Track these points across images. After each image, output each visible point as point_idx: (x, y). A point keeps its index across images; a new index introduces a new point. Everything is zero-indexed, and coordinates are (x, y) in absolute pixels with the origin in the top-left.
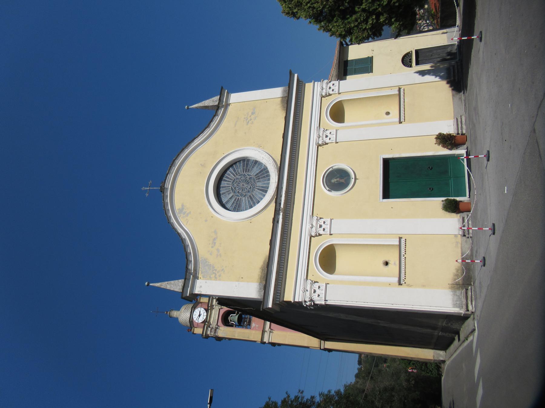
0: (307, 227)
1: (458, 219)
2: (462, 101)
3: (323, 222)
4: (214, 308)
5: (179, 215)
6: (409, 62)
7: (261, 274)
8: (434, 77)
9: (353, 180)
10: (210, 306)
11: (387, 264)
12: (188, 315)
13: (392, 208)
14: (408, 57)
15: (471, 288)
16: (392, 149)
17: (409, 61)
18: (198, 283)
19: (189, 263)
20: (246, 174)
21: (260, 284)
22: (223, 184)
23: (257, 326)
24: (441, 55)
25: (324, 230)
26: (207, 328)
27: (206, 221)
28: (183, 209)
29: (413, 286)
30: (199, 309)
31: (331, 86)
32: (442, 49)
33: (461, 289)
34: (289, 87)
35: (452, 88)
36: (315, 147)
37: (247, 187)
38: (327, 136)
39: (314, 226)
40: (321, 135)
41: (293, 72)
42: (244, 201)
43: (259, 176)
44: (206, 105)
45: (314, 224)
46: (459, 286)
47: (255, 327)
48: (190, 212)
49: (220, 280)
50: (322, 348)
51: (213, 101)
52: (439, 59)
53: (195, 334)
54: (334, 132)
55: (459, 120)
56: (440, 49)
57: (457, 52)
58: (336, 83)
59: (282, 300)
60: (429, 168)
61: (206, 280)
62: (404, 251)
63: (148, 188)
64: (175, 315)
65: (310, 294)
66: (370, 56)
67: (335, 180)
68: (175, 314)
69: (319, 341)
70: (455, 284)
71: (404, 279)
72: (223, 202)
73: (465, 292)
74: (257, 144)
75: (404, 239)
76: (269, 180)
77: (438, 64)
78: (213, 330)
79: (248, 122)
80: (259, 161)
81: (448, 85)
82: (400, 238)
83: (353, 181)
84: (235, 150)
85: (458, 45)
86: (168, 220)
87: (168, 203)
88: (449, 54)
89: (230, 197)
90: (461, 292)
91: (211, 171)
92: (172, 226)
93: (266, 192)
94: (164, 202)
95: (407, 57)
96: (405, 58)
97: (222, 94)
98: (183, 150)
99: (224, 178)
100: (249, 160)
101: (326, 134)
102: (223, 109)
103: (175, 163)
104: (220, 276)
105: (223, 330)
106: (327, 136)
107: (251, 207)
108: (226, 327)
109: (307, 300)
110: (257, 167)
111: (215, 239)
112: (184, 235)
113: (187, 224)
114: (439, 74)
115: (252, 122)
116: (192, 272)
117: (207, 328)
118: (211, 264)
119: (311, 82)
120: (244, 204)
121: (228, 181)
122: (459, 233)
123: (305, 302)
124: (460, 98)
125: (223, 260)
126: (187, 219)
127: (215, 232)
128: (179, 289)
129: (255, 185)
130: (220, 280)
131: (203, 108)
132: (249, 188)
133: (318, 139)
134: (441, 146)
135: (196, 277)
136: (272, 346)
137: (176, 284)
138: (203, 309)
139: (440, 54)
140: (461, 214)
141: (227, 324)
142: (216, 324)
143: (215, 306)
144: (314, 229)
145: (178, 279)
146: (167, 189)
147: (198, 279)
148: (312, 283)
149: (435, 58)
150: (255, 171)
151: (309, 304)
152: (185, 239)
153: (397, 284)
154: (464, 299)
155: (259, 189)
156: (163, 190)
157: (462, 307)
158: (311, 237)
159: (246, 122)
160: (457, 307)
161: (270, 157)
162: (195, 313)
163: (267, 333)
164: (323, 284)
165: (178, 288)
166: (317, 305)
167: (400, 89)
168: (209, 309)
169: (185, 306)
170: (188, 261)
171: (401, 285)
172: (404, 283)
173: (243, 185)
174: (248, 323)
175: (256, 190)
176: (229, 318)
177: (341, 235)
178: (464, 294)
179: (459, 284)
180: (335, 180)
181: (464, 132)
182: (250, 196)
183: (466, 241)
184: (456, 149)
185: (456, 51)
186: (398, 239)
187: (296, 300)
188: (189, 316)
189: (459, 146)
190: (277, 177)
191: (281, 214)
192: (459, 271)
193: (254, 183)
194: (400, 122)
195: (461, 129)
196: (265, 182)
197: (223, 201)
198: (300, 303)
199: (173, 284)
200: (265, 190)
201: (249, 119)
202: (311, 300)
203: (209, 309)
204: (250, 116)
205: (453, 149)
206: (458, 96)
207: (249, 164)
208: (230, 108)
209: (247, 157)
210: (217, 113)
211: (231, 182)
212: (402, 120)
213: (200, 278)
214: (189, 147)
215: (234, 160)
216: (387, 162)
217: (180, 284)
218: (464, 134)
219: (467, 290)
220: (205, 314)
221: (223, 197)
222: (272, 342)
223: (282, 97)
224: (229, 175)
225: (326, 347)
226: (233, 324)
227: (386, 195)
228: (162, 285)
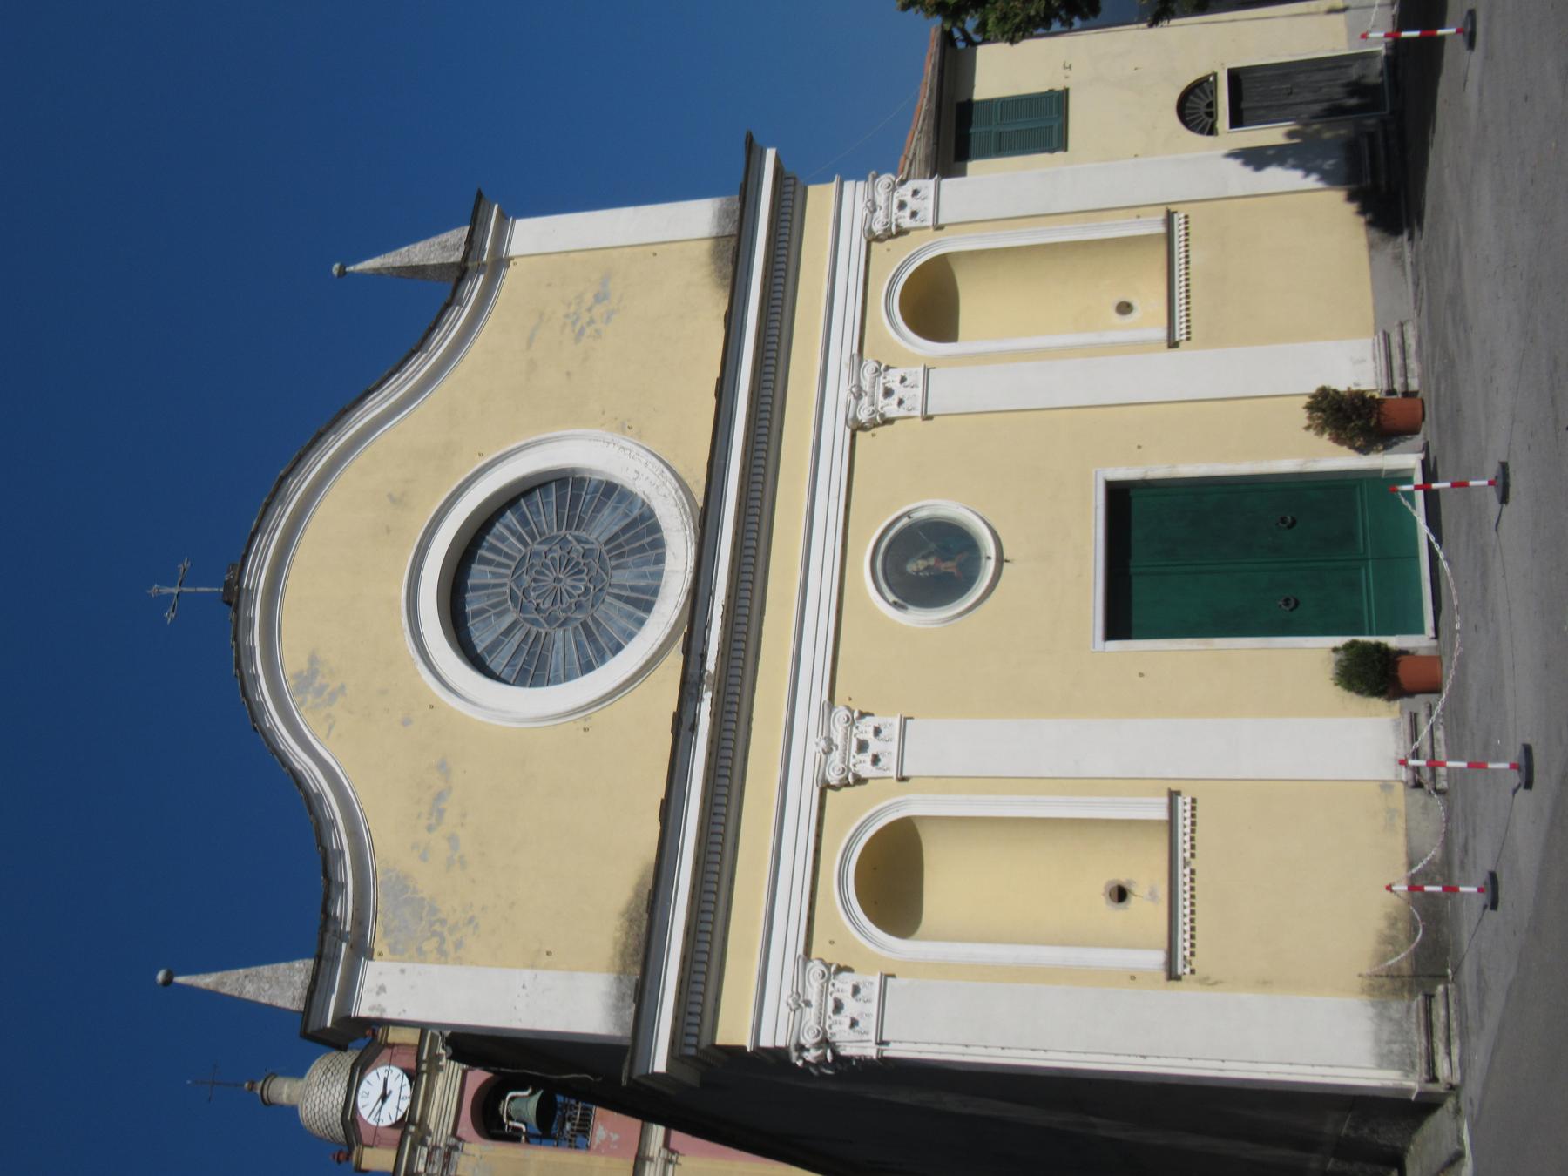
0: (807, 746)
1: (1395, 720)
2: (1403, 267)
3: (871, 730)
4: (440, 1069)
5: (298, 699)
6: (1204, 116)
7: (624, 939)
8: (1298, 174)
9: (989, 567)
10: (425, 1057)
11: (1121, 894)
12: (338, 1094)
13: (1141, 675)
14: (1202, 95)
15: (1446, 990)
16: (1139, 447)
17: (1203, 109)
18: (373, 974)
19: (333, 896)
20: (570, 538)
21: (621, 980)
22: (479, 574)
23: (615, 1137)
24: (1324, 90)
25: (876, 760)
26: (413, 1149)
27: (406, 722)
28: (313, 673)
29: (1221, 982)
30: (382, 1071)
31: (908, 198)
32: (1330, 69)
33: (1406, 994)
34: (743, 200)
35: (1369, 216)
36: (843, 434)
37: (573, 587)
38: (888, 393)
39: (837, 746)
40: (866, 385)
41: (757, 140)
42: (559, 644)
43: (620, 546)
44: (416, 261)
45: (838, 738)
46: (1397, 984)
47: (607, 1140)
48: (343, 687)
49: (459, 961)
51: (444, 248)
52: (1316, 108)
54: (916, 374)
55: (1395, 339)
56: (1321, 70)
57: (1382, 84)
58: (927, 186)
59: (709, 1043)
60: (1283, 520)
61: (404, 961)
62: (1187, 846)
63: (175, 590)
65: (820, 1018)
66: (1059, 87)
67: (921, 564)
68: (284, 1090)
70: (1384, 973)
71: (1188, 958)
72: (474, 648)
73: (1421, 1005)
74: (616, 419)
75: (1188, 800)
76: (660, 559)
77: (1316, 127)
78: (438, 1156)
79: (581, 332)
80: (622, 486)
81: (1352, 208)
82: (1173, 795)
83: (989, 567)
84: (529, 440)
85: (1387, 57)
86: (254, 720)
87: (252, 649)
88: (1356, 88)
89: (505, 626)
90: (1409, 1008)
91: (428, 521)
92: (267, 740)
93: (648, 607)
94: (238, 645)
95: (1200, 98)
96: (1191, 97)
97: (478, 222)
98: (318, 438)
99: (482, 552)
100: (582, 480)
101: (887, 385)
102: (482, 277)
103: (286, 488)
104: (459, 945)
105: (478, 1155)
106: (888, 393)
107: (588, 668)
109: (808, 1039)
110: (615, 509)
111: (440, 797)
112: (317, 780)
113: (328, 735)
114: (1319, 162)
115: (597, 331)
116: (348, 928)
117: (413, 1149)
118: (423, 899)
119: (830, 180)
120: (562, 655)
121: (499, 565)
122: (1396, 775)
123: (801, 1048)
124: (1398, 258)
125: (474, 881)
126: (329, 716)
127: (443, 768)
128: (294, 999)
129: (603, 580)
130: (461, 964)
131: (403, 274)
132: (580, 592)
133: (853, 401)
134: (1326, 436)
135: (362, 951)
137: (281, 979)
138: (396, 1072)
139: (1321, 88)
140: (1406, 701)
141: (495, 1131)
144: (836, 756)
145: (289, 957)
146: (251, 593)
147: (370, 958)
148: (829, 973)
149: (1301, 103)
150: (606, 524)
151: (816, 1058)
152: (319, 797)
153: (1163, 975)
154: (1419, 1034)
155: (618, 597)
156: (234, 597)
157: (1413, 1065)
158: (825, 787)
159: (573, 331)
160: (1391, 1066)
161: (665, 470)
162: (364, 1087)
163: (653, 1165)
164: (871, 978)
165: (290, 994)
166: (848, 1059)
167: (1169, 218)
169: (326, 1061)
170: (329, 887)
171: (1177, 978)
172: (1187, 970)
173: (557, 580)
174: (579, 1125)
175: (609, 599)
176: (504, 1108)
177: (943, 783)
178: (1418, 1017)
179: (1398, 976)
180: (920, 562)
181: (1414, 385)
182: (584, 624)
183: (1425, 807)
184: (1386, 448)
185: (1379, 80)
186: (1165, 800)
187: (766, 1042)
188: (341, 1099)
189: (1394, 440)
190: (692, 550)
191: (707, 696)
192: (1400, 925)
193: (600, 570)
194: (1173, 344)
195: (1401, 376)
196: (646, 569)
197: (476, 642)
198: (778, 1057)
199: (269, 980)
200: (643, 602)
201: (585, 318)
202: (825, 1042)
203: (423, 1072)
204: (589, 310)
205: (1372, 450)
206: (1389, 249)
207: (581, 495)
208: (510, 276)
209: (573, 470)
210: (457, 296)
211: (508, 567)
212: (1180, 334)
213: (380, 954)
214: (341, 427)
215: (523, 480)
216: (1120, 496)
217: (296, 978)
218: (1414, 394)
219: (1429, 997)
220: (407, 1091)
221: (477, 629)
223: (714, 234)
224: (503, 539)
226: (519, 1130)
227: (1119, 624)
228: (224, 984)
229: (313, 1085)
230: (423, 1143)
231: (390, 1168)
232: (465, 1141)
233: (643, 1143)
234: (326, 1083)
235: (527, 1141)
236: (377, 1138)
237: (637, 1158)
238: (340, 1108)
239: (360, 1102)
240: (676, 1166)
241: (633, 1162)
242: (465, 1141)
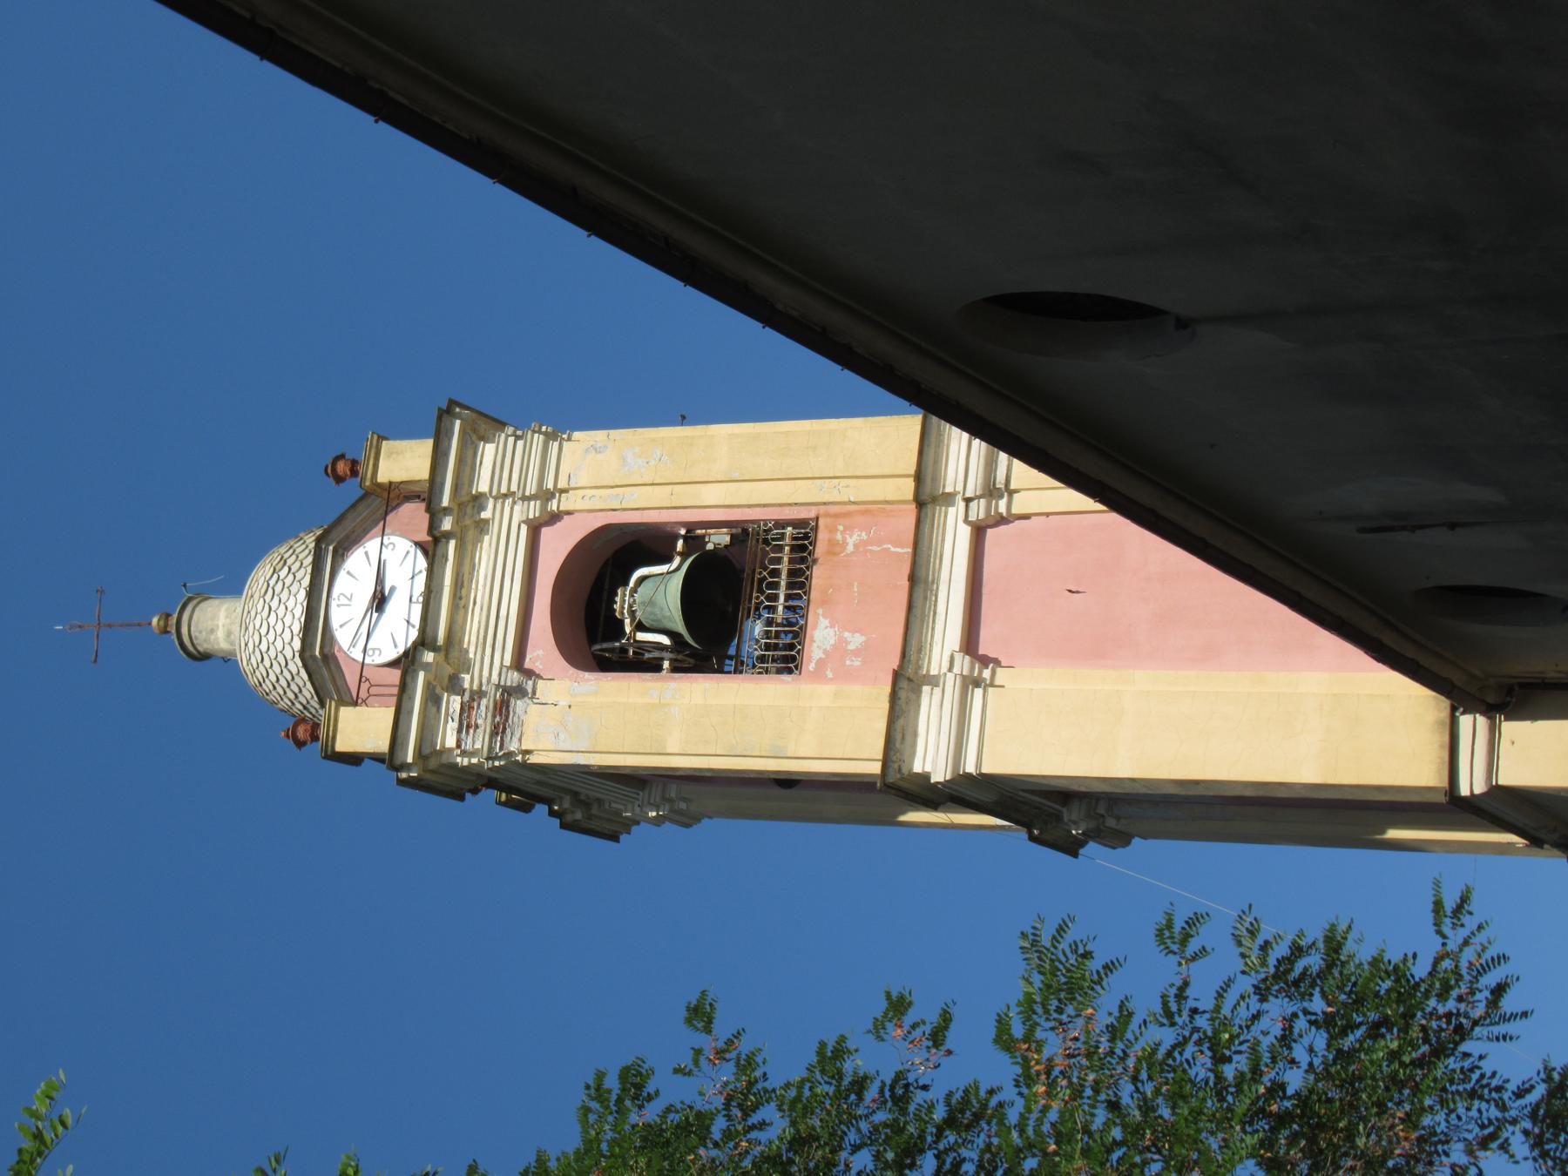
4: (482, 527)
10: (445, 502)
23: (856, 640)
26: (432, 699)
30: (372, 545)
50: (1472, 783)
53: (354, 759)
64: (221, 634)
69: (1440, 723)
78: (483, 714)
105: (563, 703)
108: (587, 675)
117: (432, 699)
136: (1032, 838)
142: (508, 660)
143: (491, 501)
162: (342, 579)
163: (937, 691)
168: (448, 536)
176: (623, 601)
203: (448, 536)
222: (984, 770)
225: (1509, 776)
229: (256, 596)
230: (454, 685)
231: (381, 744)
232: (539, 677)
233: (914, 643)
234: (278, 588)
235: (675, 669)
236: (365, 686)
237: (897, 676)
238: (296, 628)
239: (337, 617)
240: (990, 690)
242: (539, 677)
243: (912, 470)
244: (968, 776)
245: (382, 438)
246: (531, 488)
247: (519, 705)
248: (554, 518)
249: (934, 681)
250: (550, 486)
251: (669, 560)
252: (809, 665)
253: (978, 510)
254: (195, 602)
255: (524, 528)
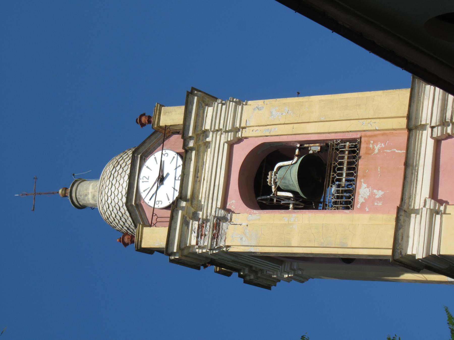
4: (207, 145)
10: (190, 134)
23: (379, 194)
26: (185, 223)
30: (158, 154)
53: (150, 251)
64: (90, 196)
78: (208, 230)
105: (244, 224)
108: (255, 211)
117: (185, 223)
142: (219, 205)
143: (211, 133)
162: (145, 172)
163: (418, 216)
168: (192, 149)
176: (271, 178)
203: (192, 149)
222: (442, 253)
230: (195, 217)
231: (162, 244)
232: (233, 212)
235: (295, 208)
236: (155, 218)
237: (399, 209)
238: (124, 192)
240: (444, 215)
241: (394, 216)
242: (233, 212)
243: (406, 114)
244: (434, 256)
245: (162, 106)
246: (229, 127)
247: (224, 225)
248: (240, 140)
249: (417, 212)
250: (238, 126)
251: (292, 159)
252: (358, 205)
253: (438, 132)
254: (78, 182)
255: (226, 145)
